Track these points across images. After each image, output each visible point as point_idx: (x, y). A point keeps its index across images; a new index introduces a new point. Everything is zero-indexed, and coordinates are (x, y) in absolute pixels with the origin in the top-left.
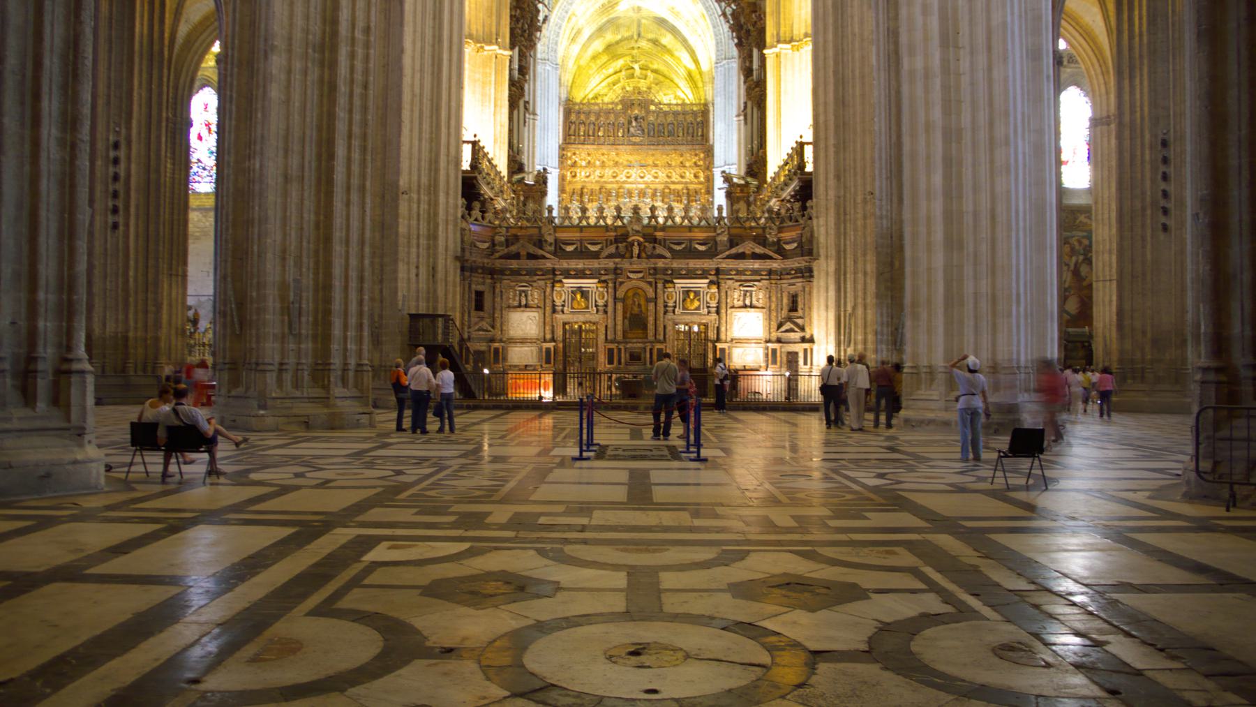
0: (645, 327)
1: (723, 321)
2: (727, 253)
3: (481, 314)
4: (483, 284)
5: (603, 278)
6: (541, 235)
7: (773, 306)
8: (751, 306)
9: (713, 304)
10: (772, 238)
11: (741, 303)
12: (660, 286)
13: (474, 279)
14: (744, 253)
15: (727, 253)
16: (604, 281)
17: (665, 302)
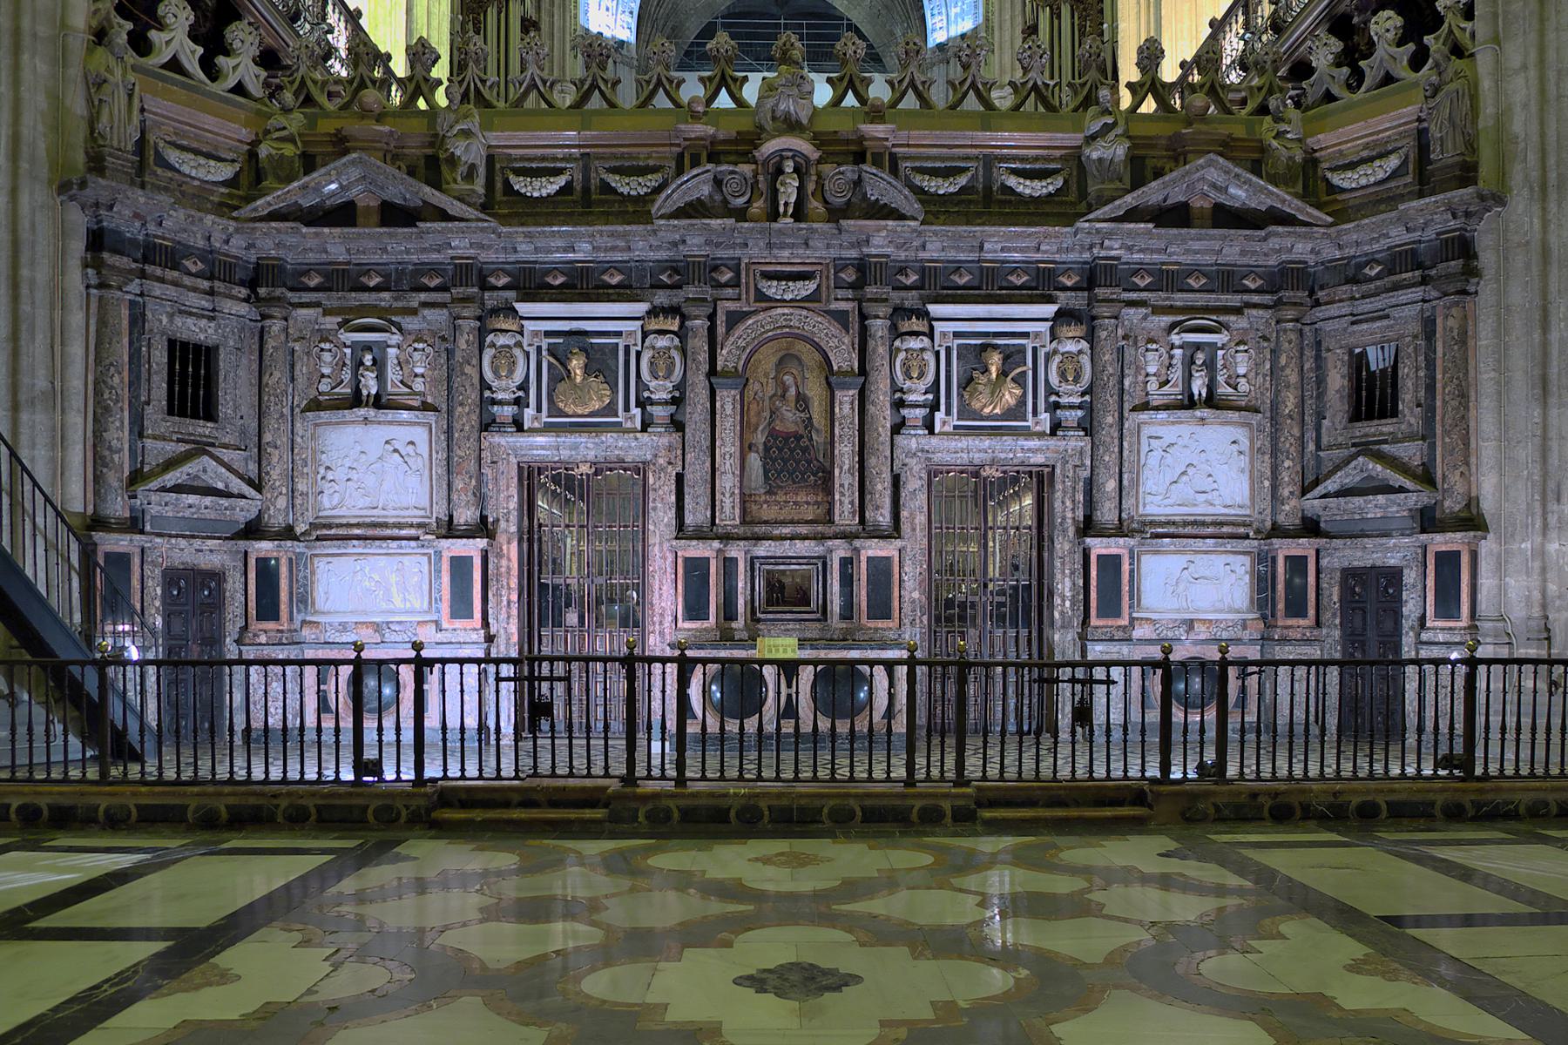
0: (826, 483)
1: (1110, 458)
2: (1130, 200)
3: (203, 428)
4: (212, 315)
5: (662, 298)
6: (437, 141)
7: (1290, 402)
8: (1212, 401)
9: (1071, 395)
10: (1285, 152)
11: (1174, 390)
12: (879, 327)
13: (157, 289)
14: (1185, 206)
15: (1130, 200)
16: (673, 311)
17: (895, 388)
